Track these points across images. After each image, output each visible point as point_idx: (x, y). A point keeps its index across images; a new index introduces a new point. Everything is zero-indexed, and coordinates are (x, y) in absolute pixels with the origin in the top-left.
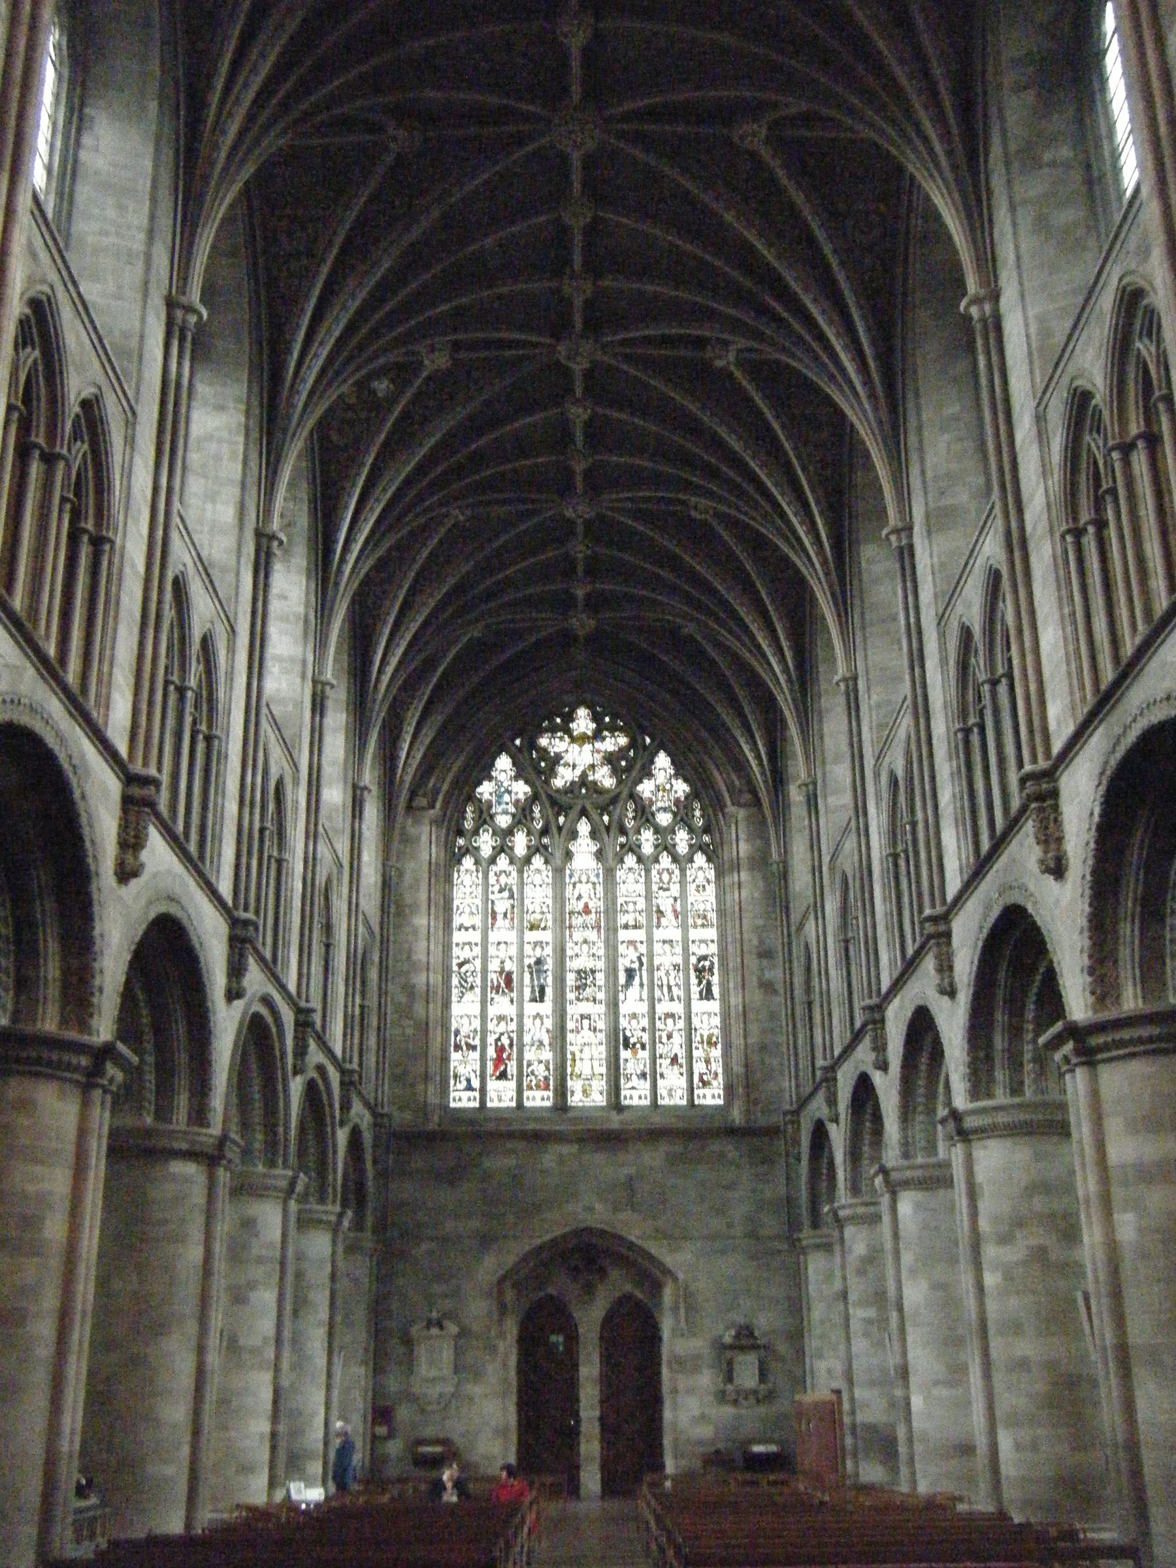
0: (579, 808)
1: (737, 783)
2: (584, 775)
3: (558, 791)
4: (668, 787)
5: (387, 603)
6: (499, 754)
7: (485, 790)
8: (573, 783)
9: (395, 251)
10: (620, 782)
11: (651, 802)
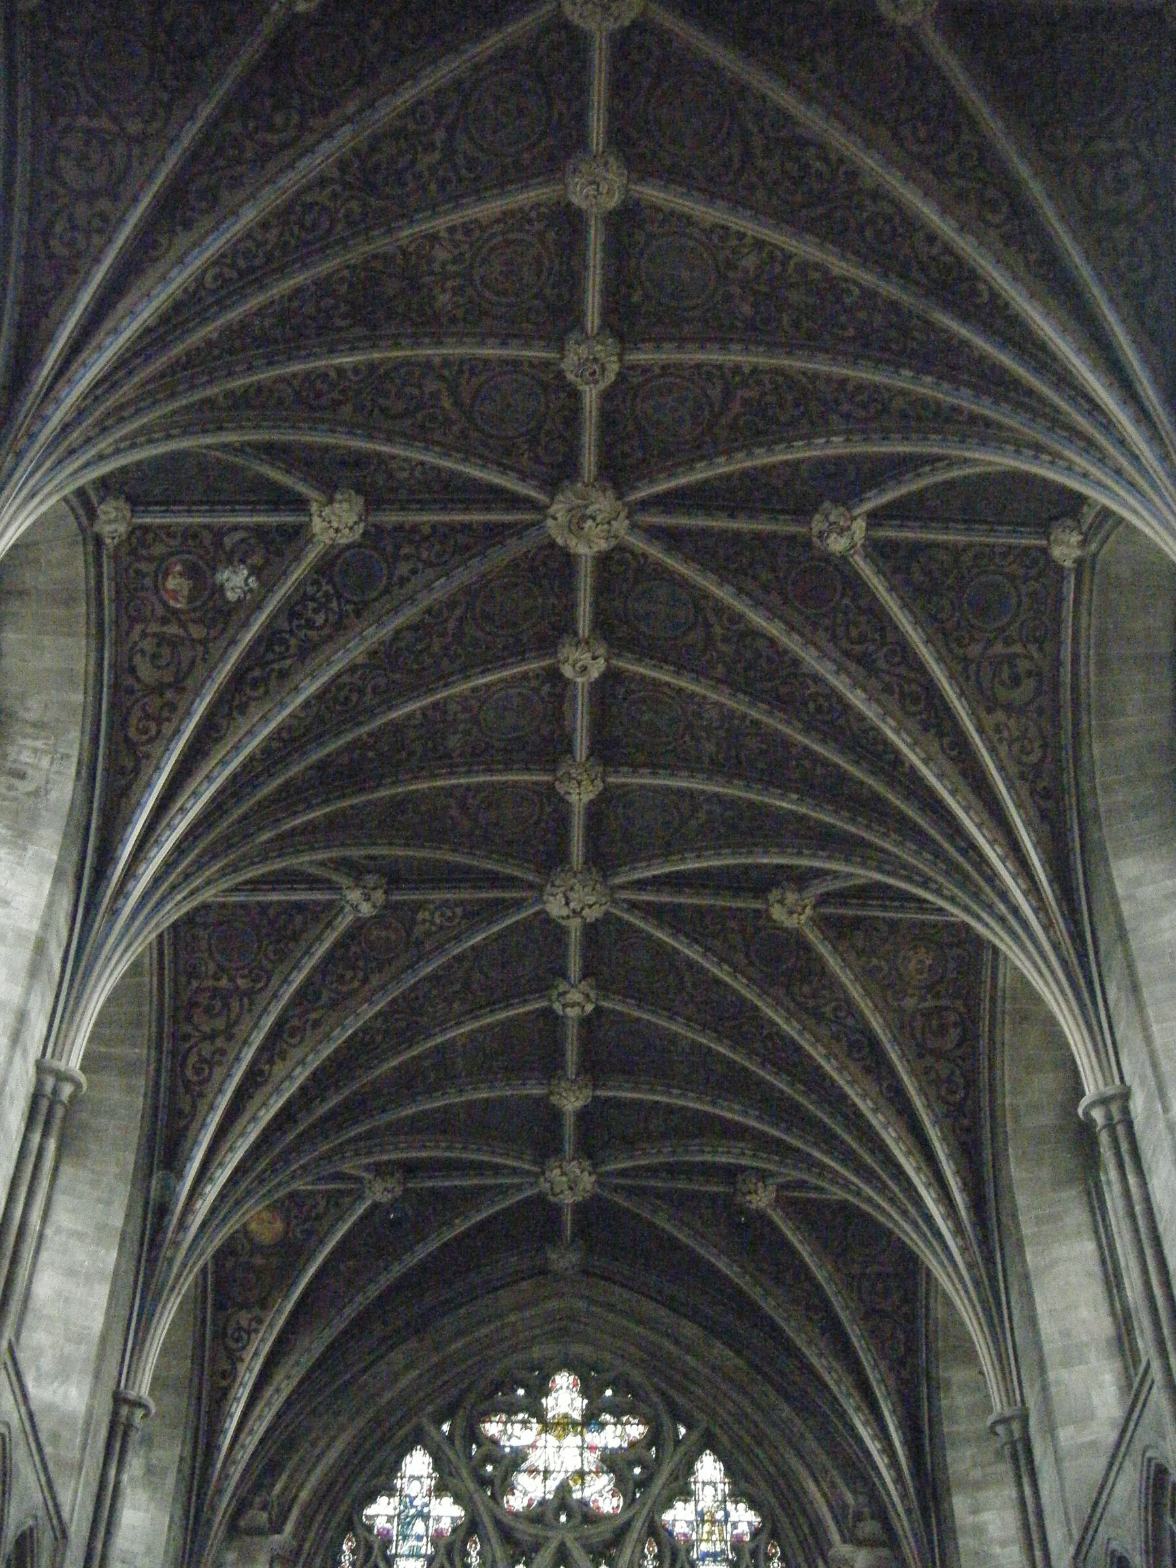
0: (553, 1545)
1: (850, 1498)
2: (564, 1489)
3: (516, 1515)
4: (720, 1515)
5: (218, 1072)
6: (409, 1449)
7: (381, 1511)
8: (543, 1502)
10: (630, 1502)
11: (690, 1546)
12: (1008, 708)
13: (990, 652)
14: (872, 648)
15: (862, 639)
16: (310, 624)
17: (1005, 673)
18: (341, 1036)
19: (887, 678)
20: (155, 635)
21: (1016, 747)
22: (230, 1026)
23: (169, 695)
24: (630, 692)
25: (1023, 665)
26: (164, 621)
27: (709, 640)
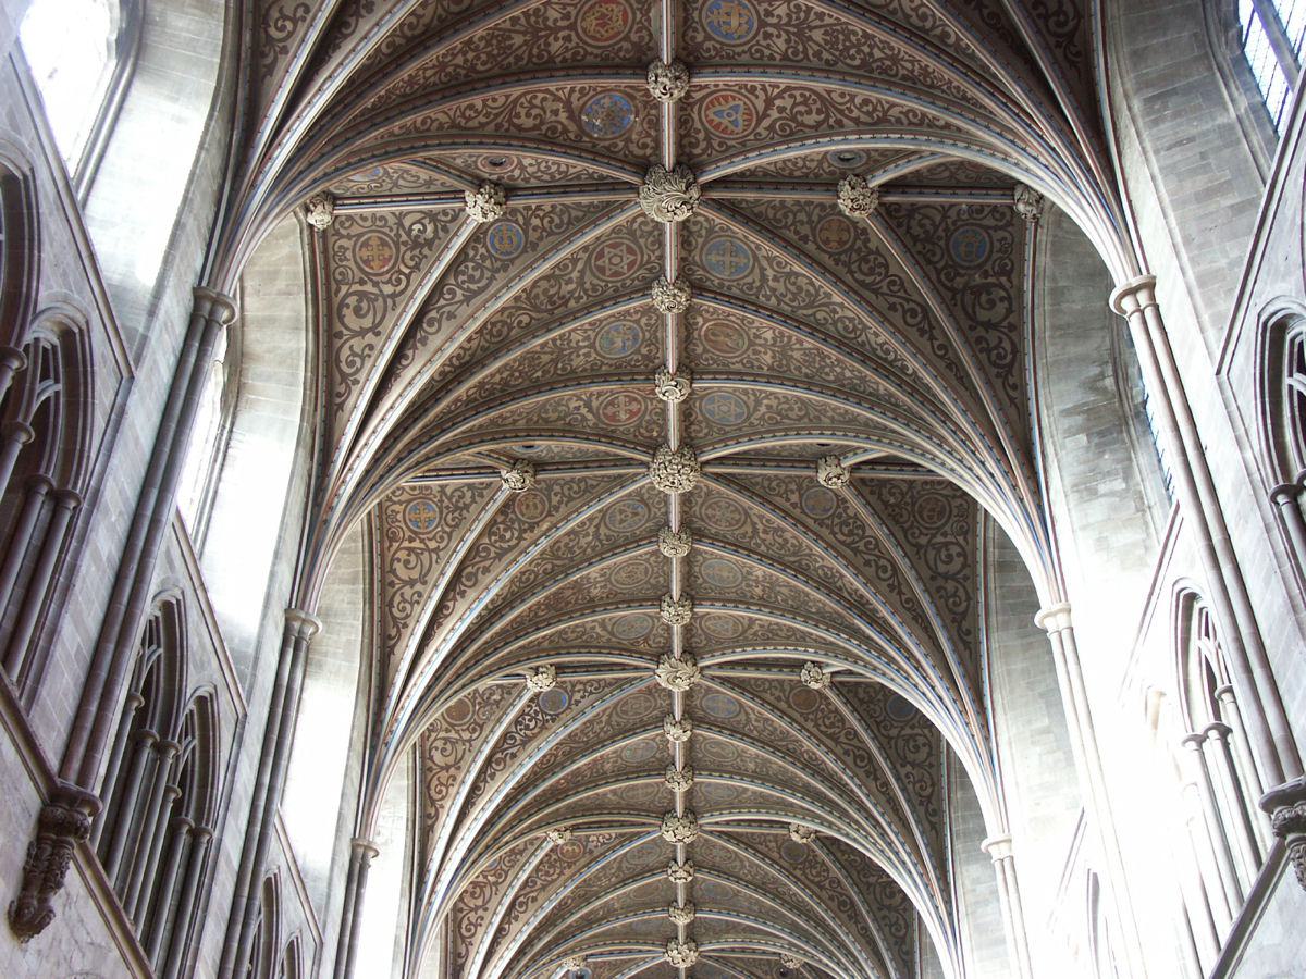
9: (505, 579)
12: (913, 765)
13: (934, 541)
14: (837, 730)
15: (832, 725)
16: (502, 538)
17: (912, 744)
18: (549, 907)
19: (846, 747)
20: (444, 738)
21: (918, 786)
22: (485, 903)
23: (452, 770)
24: (705, 559)
25: (921, 740)
26: (411, 540)
27: (755, 531)
